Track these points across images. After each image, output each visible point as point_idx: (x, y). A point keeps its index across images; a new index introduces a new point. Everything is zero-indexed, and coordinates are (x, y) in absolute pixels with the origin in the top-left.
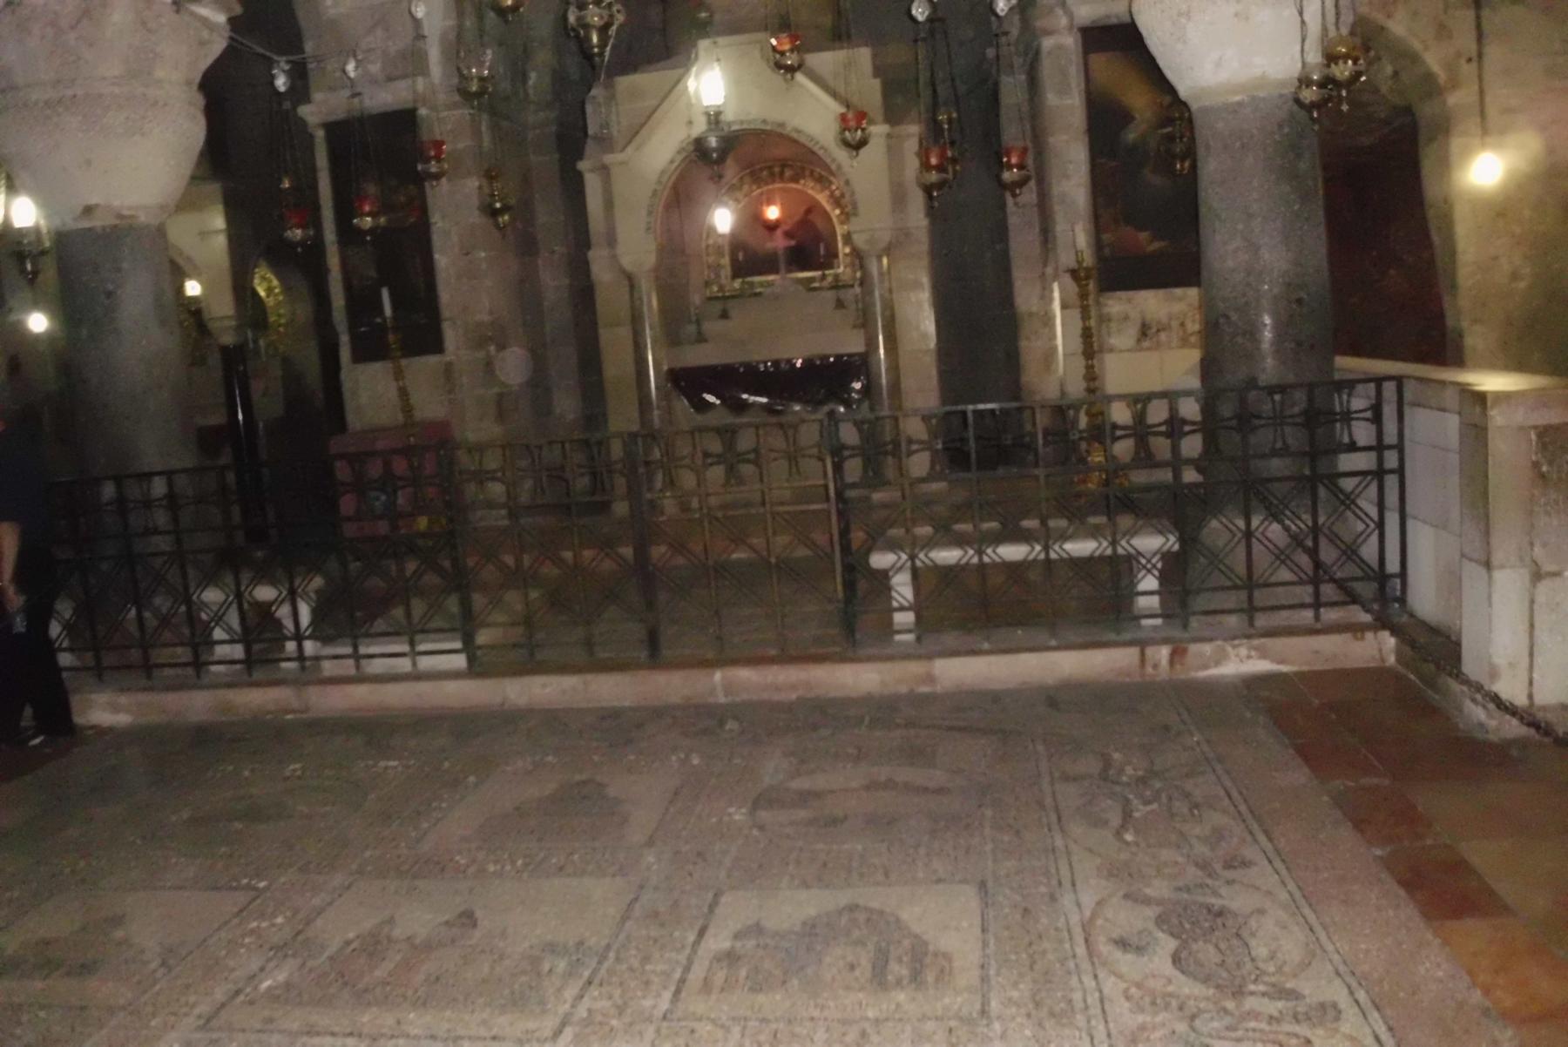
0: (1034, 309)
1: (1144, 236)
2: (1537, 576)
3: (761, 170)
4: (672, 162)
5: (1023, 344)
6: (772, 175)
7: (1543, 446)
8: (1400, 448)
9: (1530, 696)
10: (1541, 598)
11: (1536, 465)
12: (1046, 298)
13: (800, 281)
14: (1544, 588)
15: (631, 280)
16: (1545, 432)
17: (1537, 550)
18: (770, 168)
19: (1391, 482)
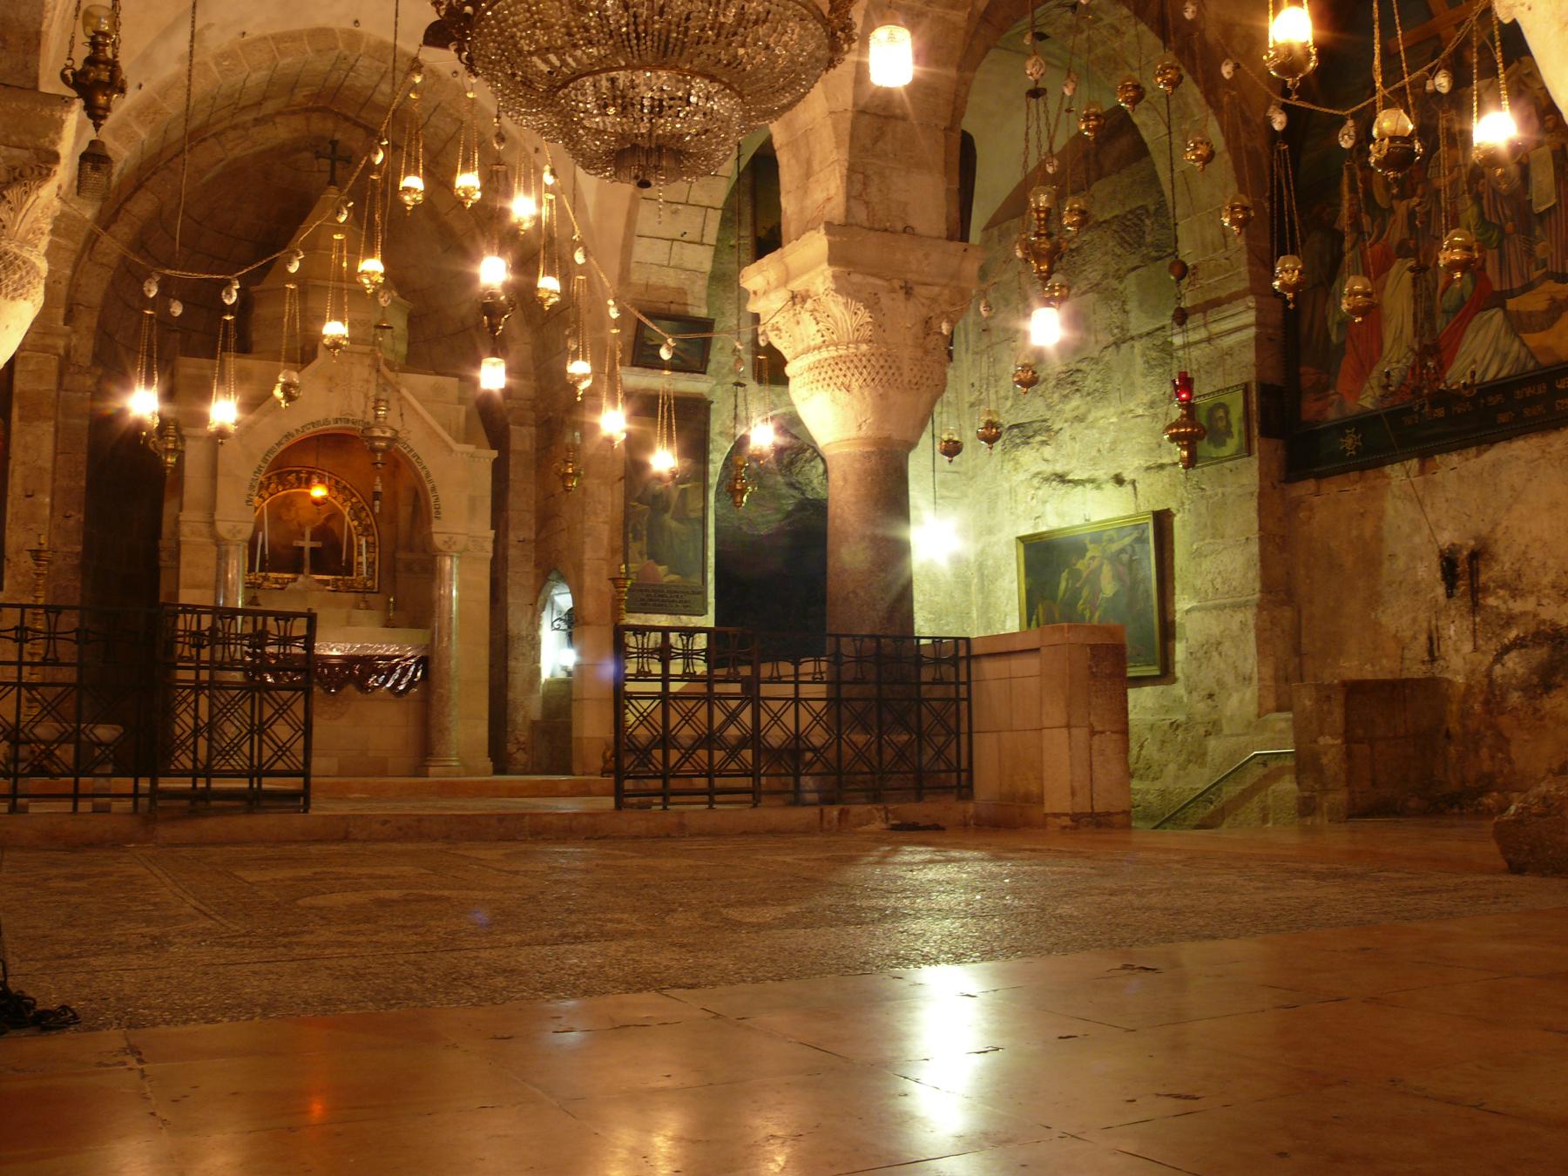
0: (524, 633)
1: (662, 569)
2: (1093, 733)
3: (290, 472)
4: (279, 444)
5: (512, 663)
6: (299, 479)
7: (1094, 656)
8: (968, 683)
9: (1092, 807)
10: (1095, 747)
11: (1090, 667)
12: (535, 625)
13: (319, 581)
14: (1096, 738)
15: (218, 541)
16: (1093, 647)
17: (1092, 718)
18: (298, 472)
19: (964, 705)
